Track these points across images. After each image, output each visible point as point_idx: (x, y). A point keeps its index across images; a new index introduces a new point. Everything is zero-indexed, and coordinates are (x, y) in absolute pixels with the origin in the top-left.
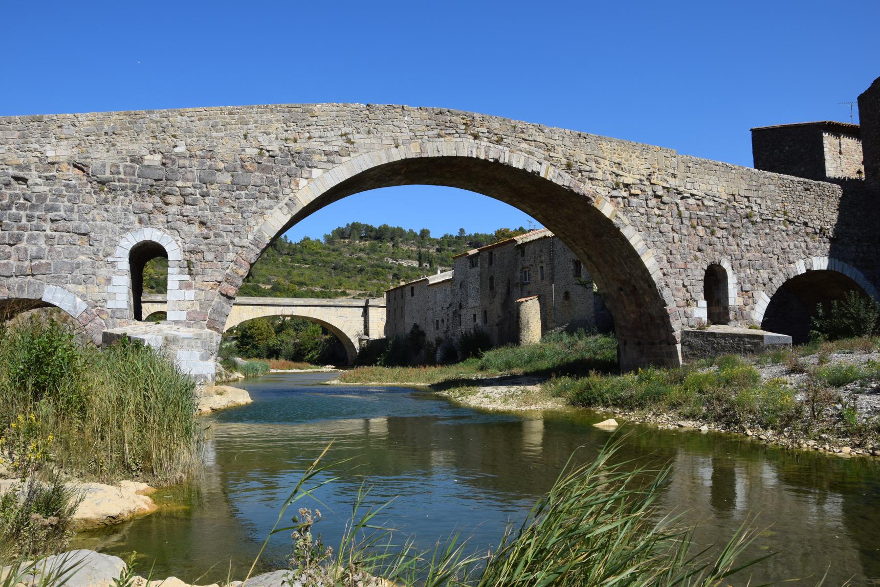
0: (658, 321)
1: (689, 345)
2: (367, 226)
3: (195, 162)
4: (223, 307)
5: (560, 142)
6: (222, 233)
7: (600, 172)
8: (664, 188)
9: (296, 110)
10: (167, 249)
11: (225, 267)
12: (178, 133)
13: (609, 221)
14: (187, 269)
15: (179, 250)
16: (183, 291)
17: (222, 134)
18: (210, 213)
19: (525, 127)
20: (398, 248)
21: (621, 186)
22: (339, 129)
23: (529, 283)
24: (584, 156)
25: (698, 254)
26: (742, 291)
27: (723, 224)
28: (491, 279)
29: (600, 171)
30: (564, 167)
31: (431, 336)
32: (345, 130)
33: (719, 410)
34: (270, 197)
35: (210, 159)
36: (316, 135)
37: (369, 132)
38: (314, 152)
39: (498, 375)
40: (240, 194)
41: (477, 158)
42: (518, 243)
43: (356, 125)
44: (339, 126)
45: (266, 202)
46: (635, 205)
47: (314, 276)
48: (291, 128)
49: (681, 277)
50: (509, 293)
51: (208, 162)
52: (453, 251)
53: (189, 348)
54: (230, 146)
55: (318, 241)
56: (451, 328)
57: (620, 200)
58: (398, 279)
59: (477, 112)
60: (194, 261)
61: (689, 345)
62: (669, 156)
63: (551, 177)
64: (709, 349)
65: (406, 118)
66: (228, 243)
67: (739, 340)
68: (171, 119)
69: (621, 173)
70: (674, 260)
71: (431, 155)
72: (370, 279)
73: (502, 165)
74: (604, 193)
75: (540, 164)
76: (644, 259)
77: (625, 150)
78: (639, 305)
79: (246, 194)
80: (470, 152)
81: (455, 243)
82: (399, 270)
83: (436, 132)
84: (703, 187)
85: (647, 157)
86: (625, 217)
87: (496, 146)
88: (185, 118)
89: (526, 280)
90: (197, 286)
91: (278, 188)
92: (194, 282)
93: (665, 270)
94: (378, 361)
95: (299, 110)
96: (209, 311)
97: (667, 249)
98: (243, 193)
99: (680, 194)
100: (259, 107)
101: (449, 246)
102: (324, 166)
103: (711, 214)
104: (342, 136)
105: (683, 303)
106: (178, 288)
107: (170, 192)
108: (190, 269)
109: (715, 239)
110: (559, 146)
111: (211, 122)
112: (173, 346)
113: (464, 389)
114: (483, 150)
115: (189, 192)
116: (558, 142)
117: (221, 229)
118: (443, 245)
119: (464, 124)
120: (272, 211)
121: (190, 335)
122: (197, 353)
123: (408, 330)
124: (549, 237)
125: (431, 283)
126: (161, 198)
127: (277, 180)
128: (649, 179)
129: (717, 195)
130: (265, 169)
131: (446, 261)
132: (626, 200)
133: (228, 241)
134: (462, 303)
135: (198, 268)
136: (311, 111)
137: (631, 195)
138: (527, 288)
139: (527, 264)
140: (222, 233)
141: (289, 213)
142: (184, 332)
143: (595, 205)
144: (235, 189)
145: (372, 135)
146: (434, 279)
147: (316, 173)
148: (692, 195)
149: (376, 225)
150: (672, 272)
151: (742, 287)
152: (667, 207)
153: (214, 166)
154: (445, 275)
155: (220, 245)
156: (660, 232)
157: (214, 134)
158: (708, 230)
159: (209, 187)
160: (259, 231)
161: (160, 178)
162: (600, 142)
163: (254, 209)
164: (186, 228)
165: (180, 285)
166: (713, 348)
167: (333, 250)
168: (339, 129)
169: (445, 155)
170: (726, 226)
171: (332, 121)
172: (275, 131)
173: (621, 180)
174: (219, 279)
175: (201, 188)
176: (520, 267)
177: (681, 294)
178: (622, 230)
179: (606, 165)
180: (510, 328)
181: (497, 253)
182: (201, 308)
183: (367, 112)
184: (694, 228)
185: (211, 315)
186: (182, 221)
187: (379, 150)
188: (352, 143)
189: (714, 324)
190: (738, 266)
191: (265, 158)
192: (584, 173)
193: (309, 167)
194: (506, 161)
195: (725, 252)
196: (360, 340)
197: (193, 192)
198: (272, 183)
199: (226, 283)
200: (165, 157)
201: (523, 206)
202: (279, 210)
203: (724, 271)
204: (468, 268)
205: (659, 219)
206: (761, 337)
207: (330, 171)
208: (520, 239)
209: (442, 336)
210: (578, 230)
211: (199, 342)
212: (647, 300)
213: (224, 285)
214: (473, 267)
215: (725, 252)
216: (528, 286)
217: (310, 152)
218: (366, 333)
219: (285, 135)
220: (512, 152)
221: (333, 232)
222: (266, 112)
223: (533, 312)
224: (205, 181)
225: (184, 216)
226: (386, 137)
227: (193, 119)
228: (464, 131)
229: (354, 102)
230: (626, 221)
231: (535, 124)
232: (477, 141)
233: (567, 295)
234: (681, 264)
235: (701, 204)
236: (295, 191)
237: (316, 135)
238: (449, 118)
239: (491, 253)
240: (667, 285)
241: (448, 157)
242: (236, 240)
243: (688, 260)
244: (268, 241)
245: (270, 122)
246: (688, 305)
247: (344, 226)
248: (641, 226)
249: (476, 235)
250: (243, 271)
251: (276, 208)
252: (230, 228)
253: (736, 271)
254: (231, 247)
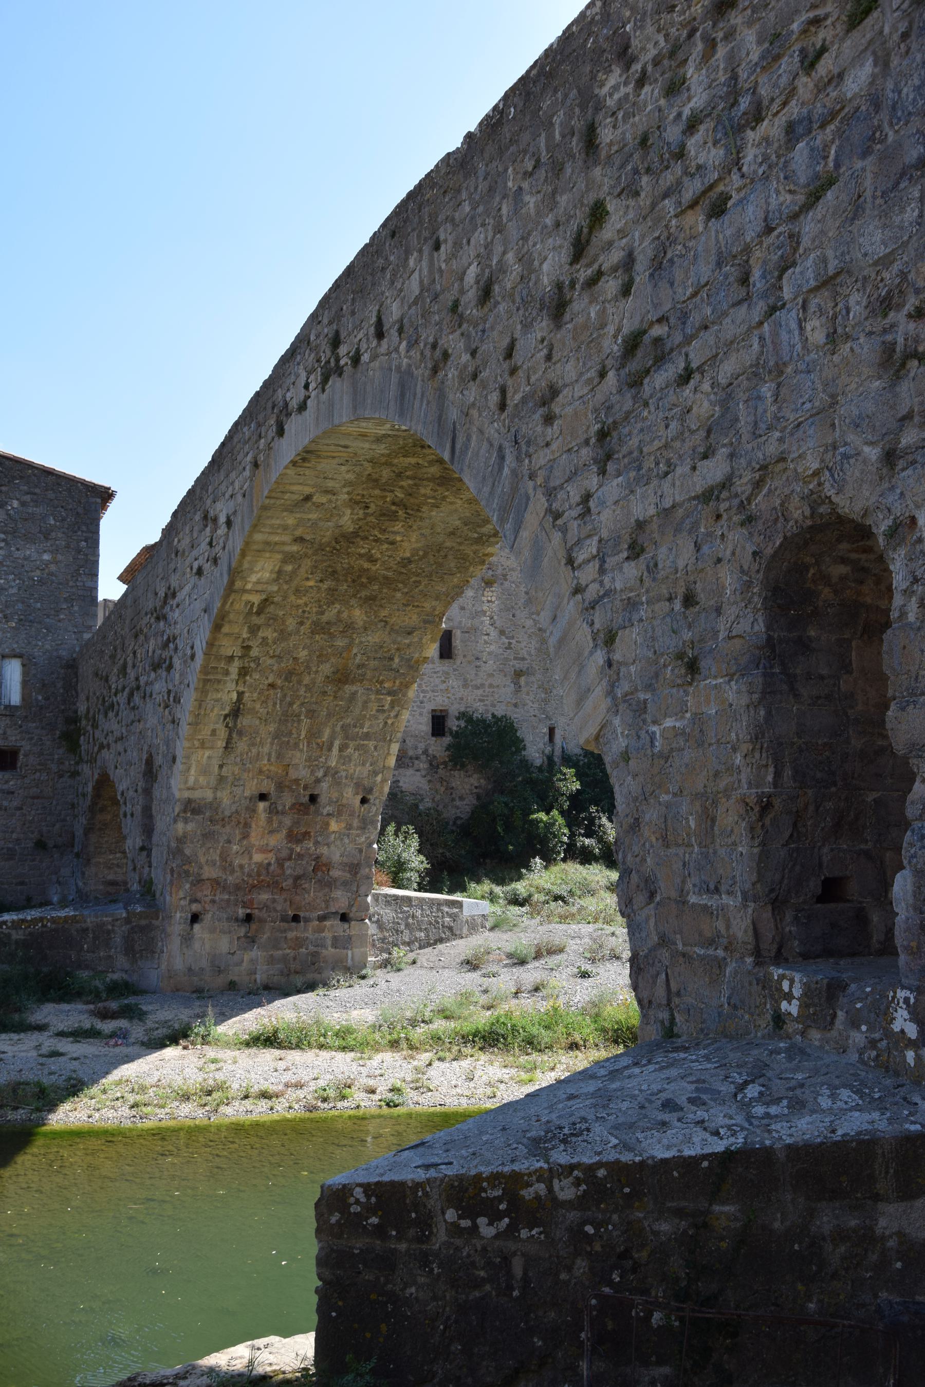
0: (335, 873)
64: (403, 927)
206: (459, 905)
212: (334, 826)
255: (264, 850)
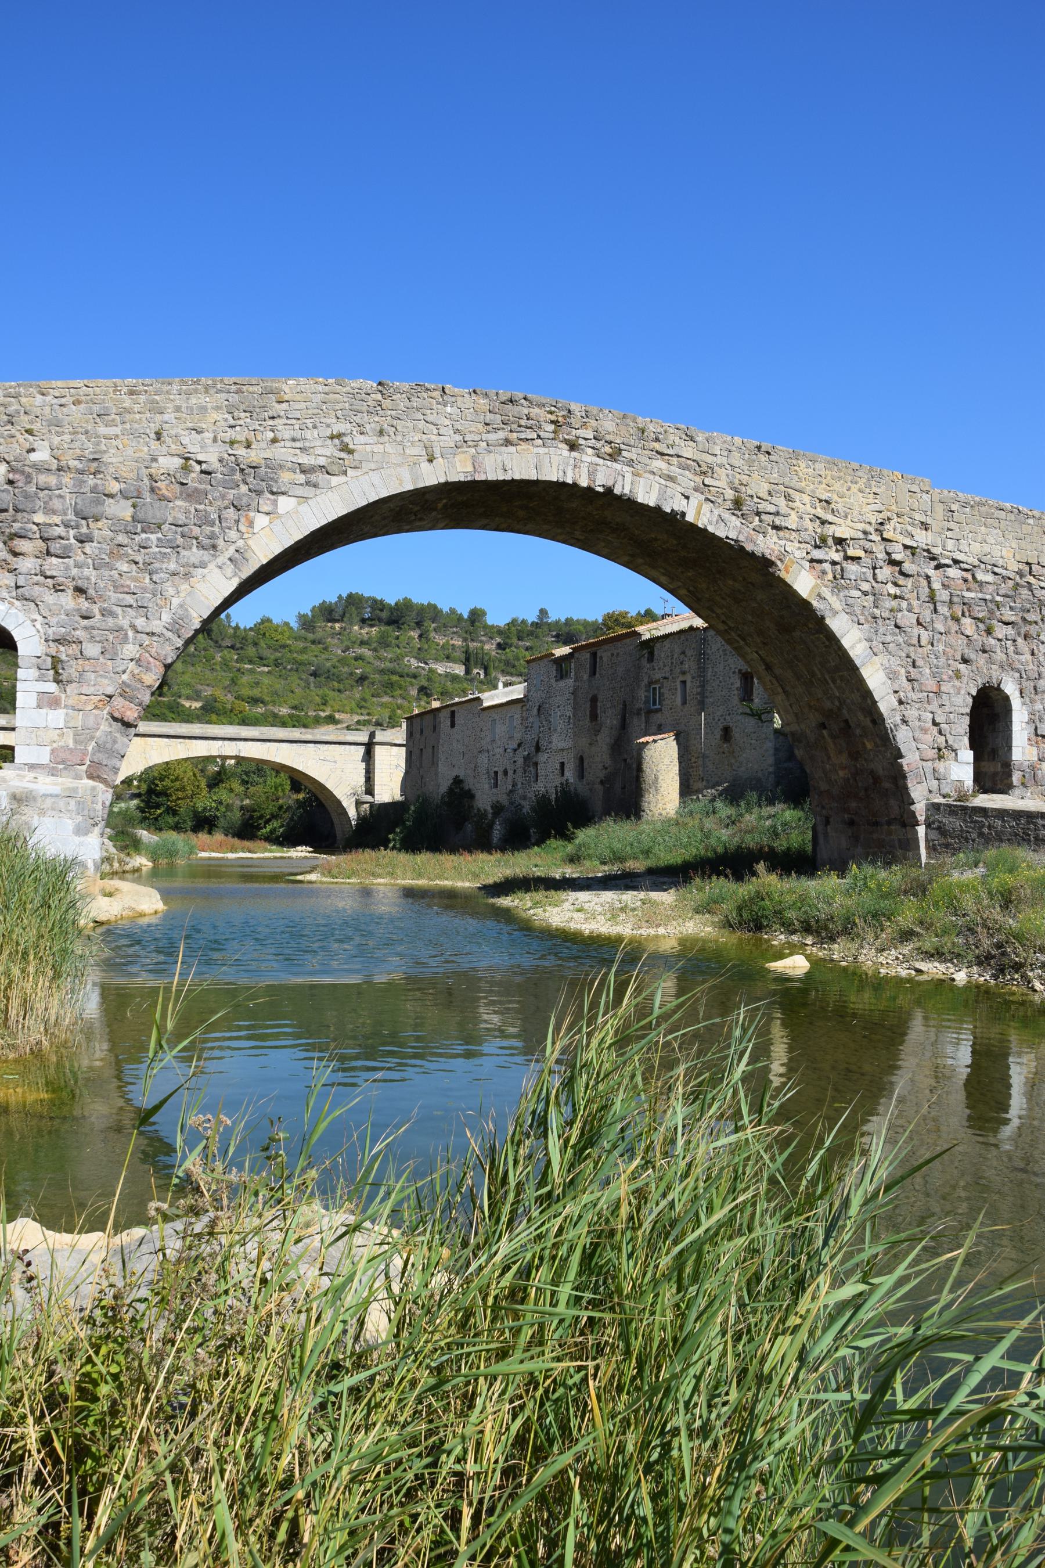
0: (887, 785)
1: (939, 828)
2: (375, 601)
3: (67, 479)
4: (115, 742)
5: (724, 460)
6: (115, 608)
7: (794, 515)
8: (906, 547)
9: (251, 389)
10: (16, 635)
11: (120, 669)
12: (36, 426)
13: (806, 604)
14: (52, 672)
15: (37, 638)
16: (44, 711)
17: (117, 430)
18: (94, 573)
19: (662, 430)
20: (428, 640)
21: (830, 541)
22: (328, 426)
23: (660, 710)
24: (766, 487)
25: (962, 667)
26: (1037, 735)
27: (1008, 615)
28: (594, 700)
29: (793, 513)
30: (729, 504)
31: (484, 798)
32: (338, 428)
33: (986, 943)
34: (201, 547)
35: (94, 474)
36: (287, 436)
37: (381, 433)
38: (281, 467)
39: (600, 872)
40: (148, 539)
41: (575, 485)
42: (644, 638)
43: (358, 419)
44: (328, 421)
45: (194, 554)
46: (853, 577)
47: (277, 686)
48: (241, 422)
49: (929, 708)
50: (624, 725)
51: (91, 481)
52: (527, 649)
53: (54, 813)
54: (130, 451)
55: (287, 624)
56: (520, 786)
57: (827, 566)
58: (428, 695)
59: (577, 401)
60: (63, 657)
61: (939, 828)
62: (917, 490)
63: (706, 521)
64: (974, 835)
65: (449, 409)
66: (126, 626)
67: (1028, 823)
68: (23, 400)
69: (830, 517)
70: (918, 677)
71: (491, 477)
72: (377, 695)
73: (619, 498)
74: (798, 554)
75: (687, 498)
76: (866, 673)
77: (840, 478)
78: (855, 755)
79: (158, 539)
80: (561, 473)
81: (531, 634)
82: (429, 680)
83: (501, 435)
84: (976, 547)
85: (878, 491)
86: (835, 598)
87: (609, 463)
88: (49, 398)
89: (654, 703)
90: (70, 702)
91: (216, 529)
92: (63, 696)
93: (902, 694)
94: (389, 841)
95: (255, 389)
96: (90, 749)
97: (908, 656)
98: (153, 537)
99: (933, 559)
100: (184, 383)
101: (520, 639)
102: (300, 491)
103: (988, 597)
104: (332, 438)
105: (932, 754)
106: (35, 705)
107: (23, 532)
108: (57, 672)
109: (992, 641)
110: (721, 466)
111: (96, 408)
112: (26, 810)
113: (540, 895)
114: (584, 471)
115: (56, 534)
116: (720, 460)
117: (113, 601)
118: (508, 637)
119: (552, 422)
120: (205, 571)
121: (56, 790)
122: (69, 821)
123: (444, 785)
124: (698, 629)
125: (486, 704)
126: (5, 543)
127: (214, 516)
128: (880, 532)
129: (1000, 562)
130: (193, 496)
131: (514, 666)
132: (838, 567)
133: (125, 623)
134: (541, 742)
135: (70, 671)
136: (276, 392)
137: (847, 558)
138: (657, 718)
139: (658, 675)
140: (115, 608)
141: (236, 574)
142: (45, 784)
143: (783, 574)
144: (139, 530)
145: (386, 438)
146: (492, 698)
147: (285, 503)
148: (956, 562)
149: (391, 600)
150: (915, 698)
151: (1036, 729)
152: (909, 583)
153: (101, 488)
154: (512, 692)
155: (112, 631)
156: (897, 626)
157: (102, 430)
158: (981, 626)
159: (91, 525)
160: (181, 606)
161: (4, 507)
162: (795, 462)
163: (173, 566)
164: (50, 598)
165: (39, 700)
166: (981, 834)
167: (313, 642)
168: (328, 426)
169: (517, 477)
170: (1013, 619)
171: (316, 411)
172: (212, 428)
173: (830, 530)
174: (110, 691)
175: (77, 527)
176: (646, 681)
177: (929, 738)
178: (828, 621)
179: (804, 503)
180: (624, 788)
181: (604, 654)
182: (76, 742)
183: (379, 397)
184: (957, 620)
185: (93, 754)
186: (43, 585)
187: (399, 465)
188: (351, 452)
189: (985, 791)
190: (1031, 691)
191: (193, 475)
192: (764, 517)
193: (273, 493)
194: (627, 491)
195: (1010, 665)
196: (359, 804)
197: (63, 534)
198: (204, 521)
199: (120, 699)
200: (12, 470)
201: (654, 573)
202: (217, 570)
203: (1007, 699)
204: (553, 681)
205: (894, 603)
207: (310, 501)
208: (646, 631)
209: (504, 800)
210: (750, 618)
211: (72, 802)
213: (118, 702)
214: (562, 678)
215: (1010, 665)
216: (659, 715)
217: (275, 466)
218: (370, 790)
219: (231, 434)
220: (638, 475)
221: (313, 610)
222: (196, 391)
223: (666, 761)
224: (85, 514)
225: (46, 577)
226: (412, 443)
227: (63, 401)
228: (552, 436)
229: (354, 377)
230: (837, 605)
231: (679, 426)
232: (574, 454)
233: (727, 733)
234: (930, 684)
235: (970, 577)
236: (246, 536)
237: (287, 436)
238: (526, 411)
239: (594, 655)
240: (905, 721)
241: (522, 481)
242: (140, 622)
243: (944, 677)
244: (197, 626)
245: (203, 409)
246: (940, 757)
247: (334, 599)
248: (862, 614)
249: (569, 622)
250: (153, 678)
251: (211, 566)
252: (130, 600)
253: (1028, 700)
254: (130, 633)
255: (843, 768)
